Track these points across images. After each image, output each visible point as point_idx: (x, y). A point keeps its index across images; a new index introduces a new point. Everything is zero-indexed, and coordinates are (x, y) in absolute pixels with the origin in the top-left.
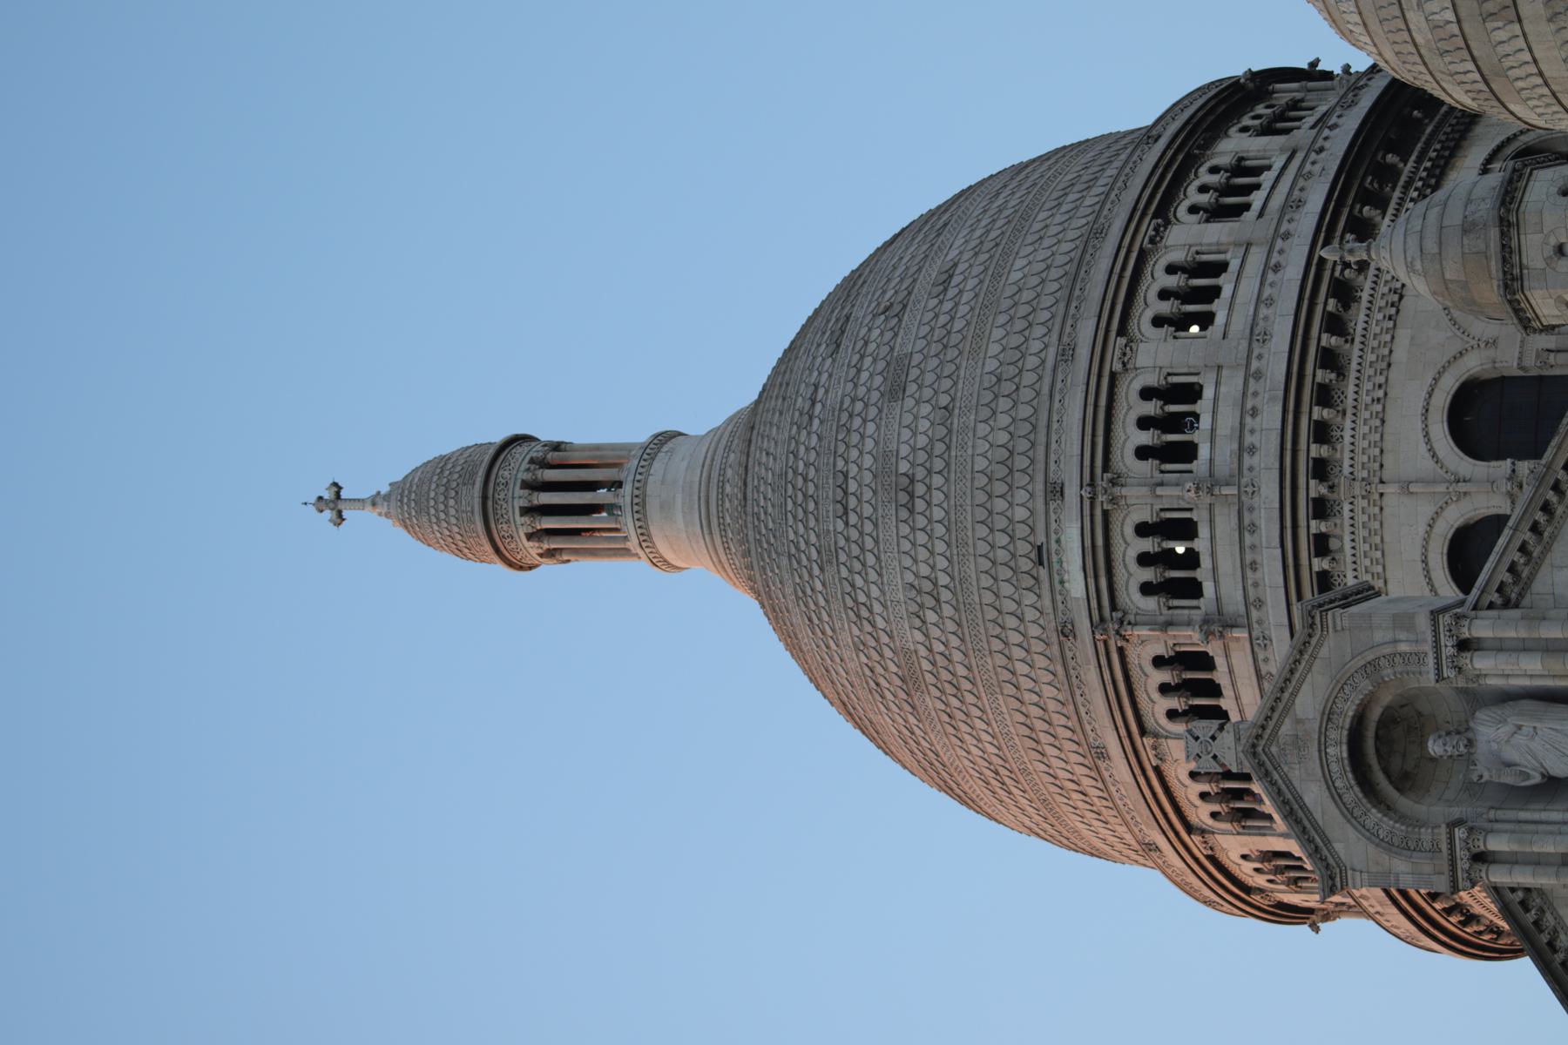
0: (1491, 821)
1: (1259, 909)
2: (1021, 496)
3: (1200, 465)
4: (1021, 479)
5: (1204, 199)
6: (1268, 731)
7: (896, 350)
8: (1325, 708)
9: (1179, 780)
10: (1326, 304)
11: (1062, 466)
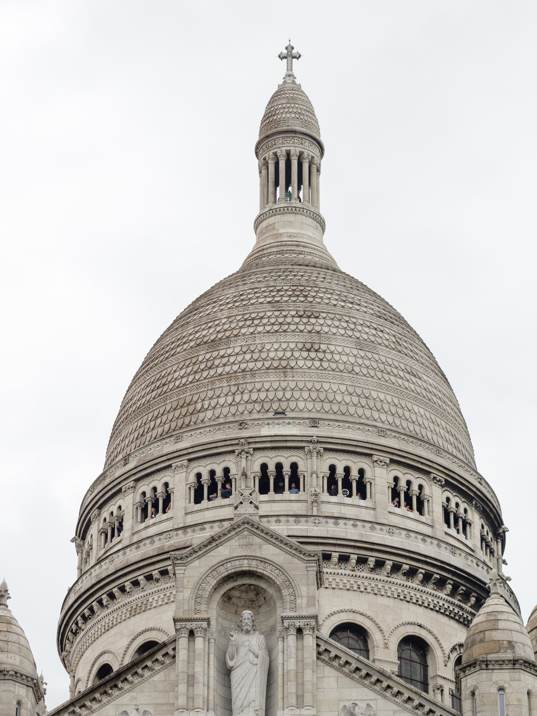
0: (209, 640)
1: (89, 513)
2: (310, 406)
3: (325, 496)
4: (318, 406)
5: (453, 505)
6: (255, 531)
7: (380, 347)
8: (267, 559)
9: (163, 477)
10: (406, 564)
11: (327, 427)
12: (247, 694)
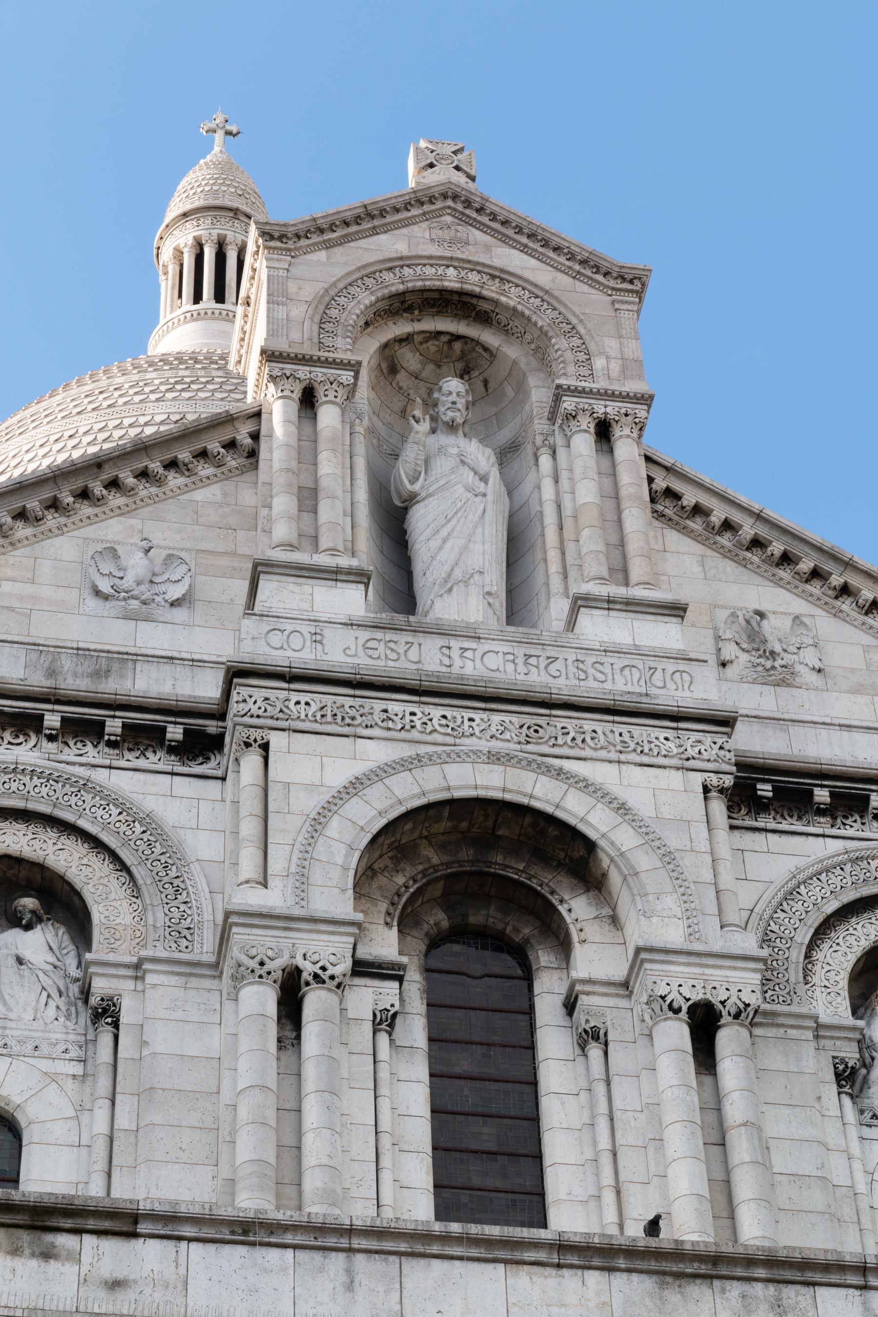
6: (474, 215)
12: (461, 554)
